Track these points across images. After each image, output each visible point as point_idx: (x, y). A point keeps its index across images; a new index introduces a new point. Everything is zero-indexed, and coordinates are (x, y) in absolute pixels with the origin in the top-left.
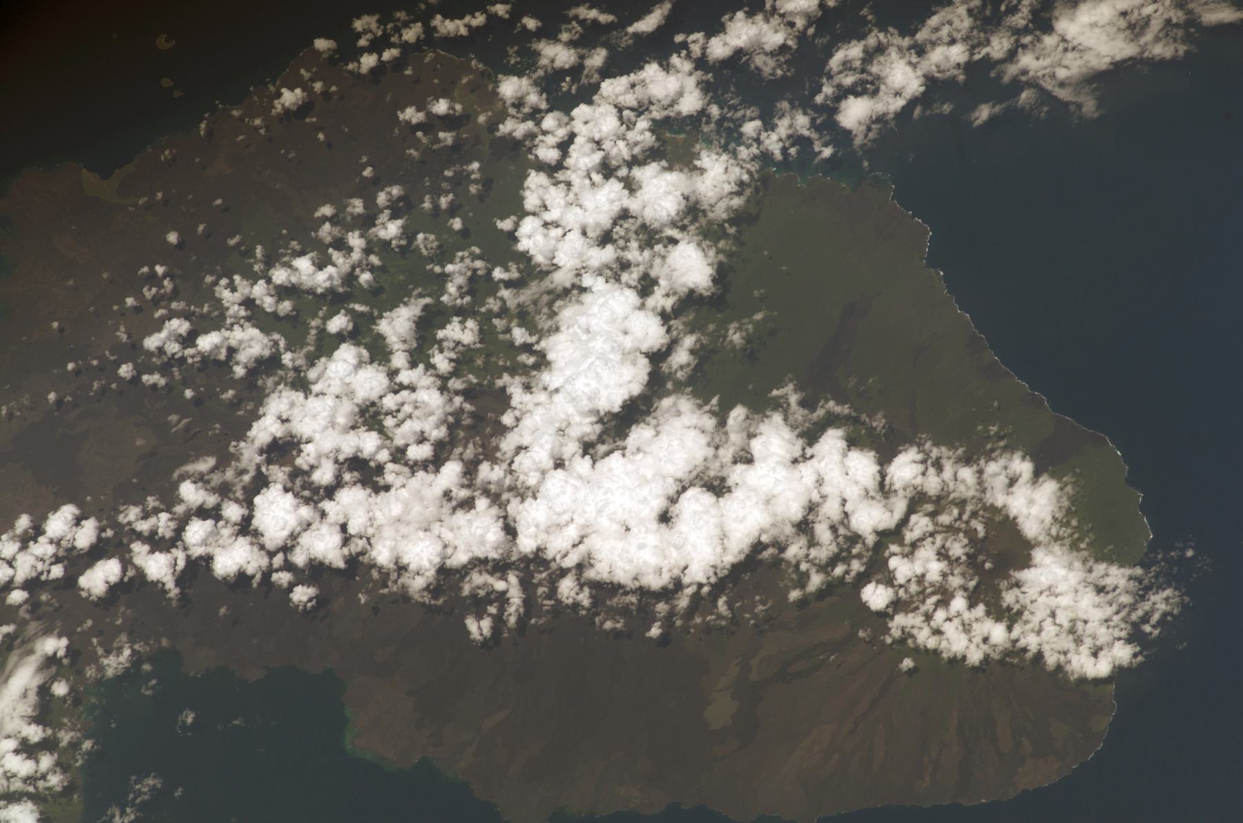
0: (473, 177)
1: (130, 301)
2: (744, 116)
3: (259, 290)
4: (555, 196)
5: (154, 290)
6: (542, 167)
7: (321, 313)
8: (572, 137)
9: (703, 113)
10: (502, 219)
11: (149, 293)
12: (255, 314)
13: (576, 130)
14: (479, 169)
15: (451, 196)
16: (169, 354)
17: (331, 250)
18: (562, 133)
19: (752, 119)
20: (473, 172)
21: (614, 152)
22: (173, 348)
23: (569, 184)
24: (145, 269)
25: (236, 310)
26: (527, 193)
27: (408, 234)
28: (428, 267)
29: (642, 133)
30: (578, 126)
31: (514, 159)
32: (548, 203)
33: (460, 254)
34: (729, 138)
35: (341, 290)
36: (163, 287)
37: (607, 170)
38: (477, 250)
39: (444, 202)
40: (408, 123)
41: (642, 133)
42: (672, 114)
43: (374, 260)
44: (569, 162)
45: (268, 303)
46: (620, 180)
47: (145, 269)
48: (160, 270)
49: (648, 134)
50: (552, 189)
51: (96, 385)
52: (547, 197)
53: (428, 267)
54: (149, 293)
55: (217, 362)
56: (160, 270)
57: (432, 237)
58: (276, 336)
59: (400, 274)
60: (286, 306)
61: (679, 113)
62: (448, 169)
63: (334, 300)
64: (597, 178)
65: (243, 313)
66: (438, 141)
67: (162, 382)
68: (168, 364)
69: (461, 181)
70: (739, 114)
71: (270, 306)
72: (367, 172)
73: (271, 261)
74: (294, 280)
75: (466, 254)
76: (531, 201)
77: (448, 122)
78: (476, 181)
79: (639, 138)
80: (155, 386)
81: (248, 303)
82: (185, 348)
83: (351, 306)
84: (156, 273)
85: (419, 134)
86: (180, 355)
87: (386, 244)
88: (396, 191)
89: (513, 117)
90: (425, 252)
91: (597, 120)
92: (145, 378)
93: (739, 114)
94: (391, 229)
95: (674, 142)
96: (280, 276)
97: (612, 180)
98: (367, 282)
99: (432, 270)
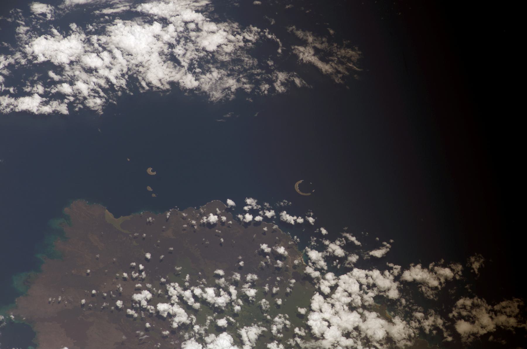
0: (291, 285)
1: (125, 275)
2: (417, 309)
3: (187, 294)
4: (326, 307)
5: (137, 274)
6: (321, 293)
7: (215, 315)
8: (337, 286)
9: (398, 300)
10: (301, 307)
11: (135, 275)
12: (182, 302)
13: (339, 284)
14: (294, 284)
15: (278, 289)
16: (142, 304)
17: (221, 290)
18: (333, 283)
19: (420, 312)
20: (291, 283)
21: (356, 301)
22: (144, 303)
23: (333, 305)
24: (134, 264)
25: (175, 299)
26: (313, 302)
27: (258, 297)
28: (265, 315)
29: (370, 297)
30: (341, 283)
31: (309, 286)
32: (323, 310)
33: (280, 315)
34: (408, 317)
35: (223, 308)
36: (141, 275)
37: (352, 308)
38: (287, 316)
39: (275, 290)
40: (263, 250)
41: (370, 297)
42: (385, 296)
43: (240, 302)
44: (334, 296)
45: (191, 301)
46: (359, 313)
47: (134, 264)
48: (141, 267)
49: (372, 299)
50: (326, 304)
51: (105, 304)
52: (323, 307)
53: (265, 315)
54: (135, 275)
55: (161, 317)
56: (141, 267)
57: (268, 303)
58: (193, 317)
59: (251, 314)
60: (197, 305)
61: (388, 296)
62: (279, 277)
63: (219, 312)
64: (346, 308)
65: (177, 300)
66: (276, 263)
67: (136, 315)
68: (140, 309)
69: (283, 285)
70: (415, 307)
71: (192, 303)
72: (241, 263)
73: (194, 283)
74: (205, 296)
75: (282, 315)
76: (315, 305)
77: (281, 257)
78: (290, 288)
79: (368, 299)
80: (132, 316)
81: (180, 297)
82: (148, 305)
83: (228, 317)
84: (139, 267)
85: (268, 257)
86: (146, 307)
87: (244, 297)
88: (255, 277)
89: (310, 267)
90: (264, 308)
91: (350, 282)
92: (129, 310)
93: (415, 307)
94: (252, 292)
95: (384, 306)
96: (198, 291)
97: (355, 312)
98: (238, 310)
99: (266, 317)
